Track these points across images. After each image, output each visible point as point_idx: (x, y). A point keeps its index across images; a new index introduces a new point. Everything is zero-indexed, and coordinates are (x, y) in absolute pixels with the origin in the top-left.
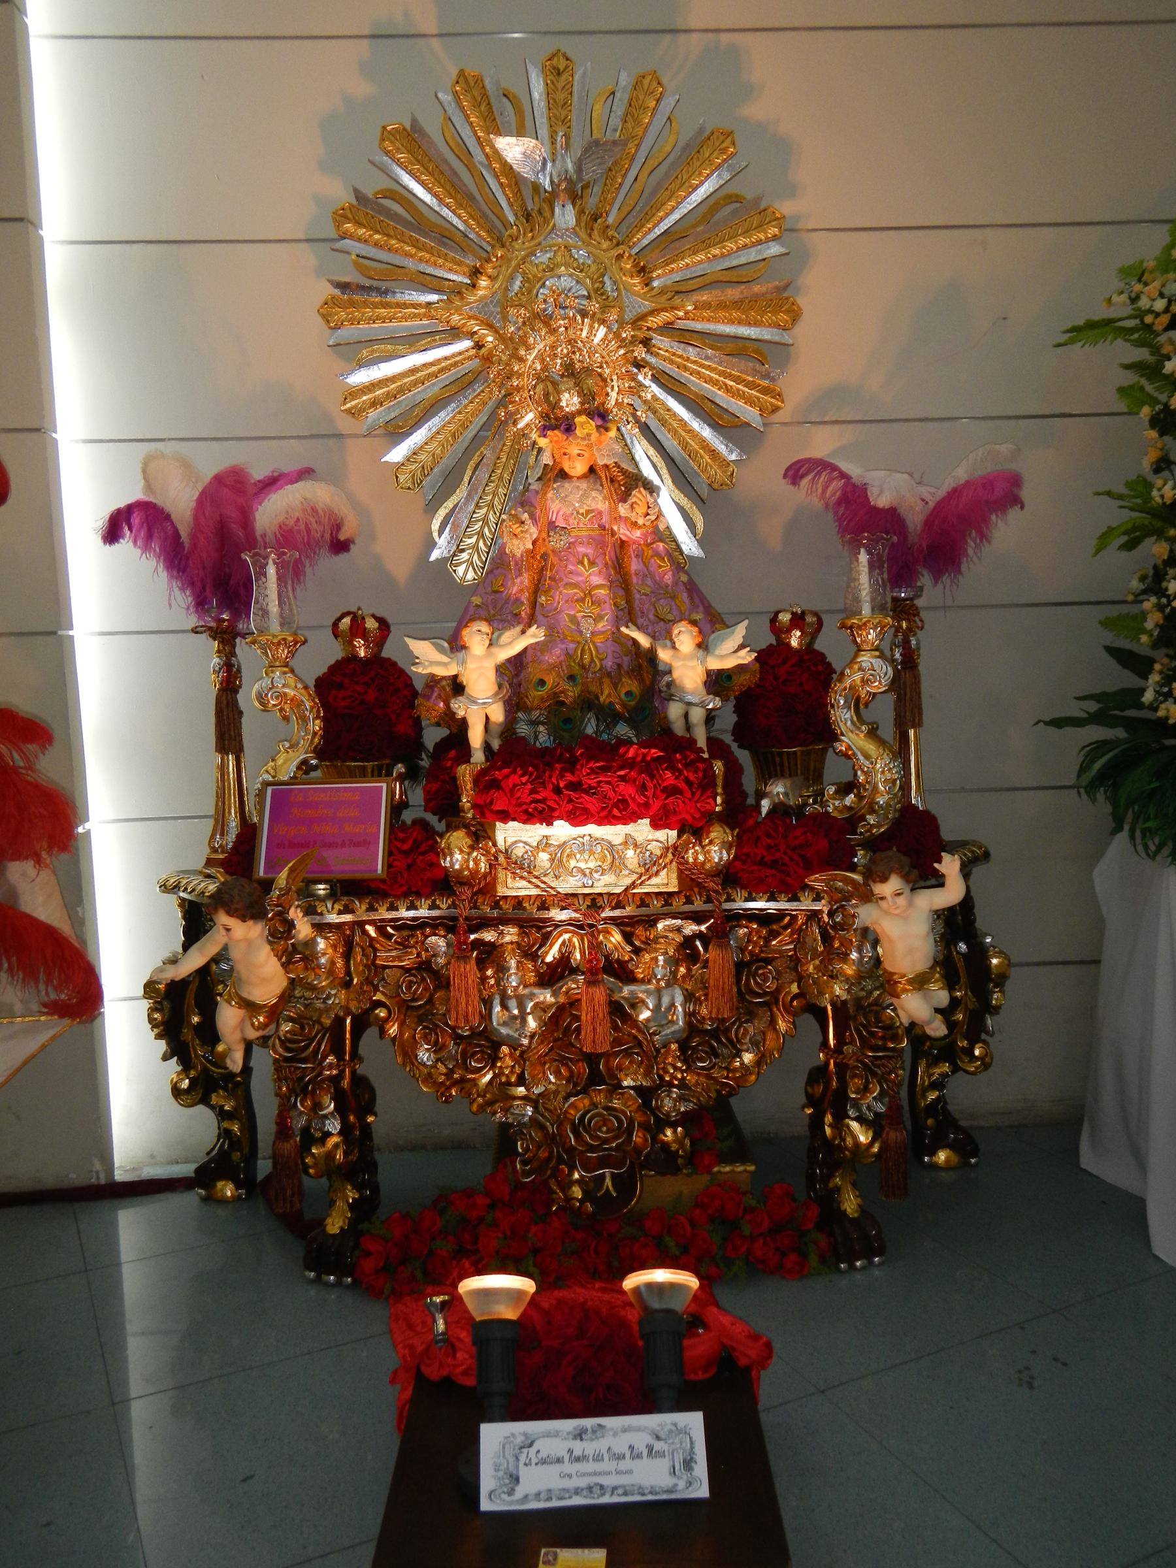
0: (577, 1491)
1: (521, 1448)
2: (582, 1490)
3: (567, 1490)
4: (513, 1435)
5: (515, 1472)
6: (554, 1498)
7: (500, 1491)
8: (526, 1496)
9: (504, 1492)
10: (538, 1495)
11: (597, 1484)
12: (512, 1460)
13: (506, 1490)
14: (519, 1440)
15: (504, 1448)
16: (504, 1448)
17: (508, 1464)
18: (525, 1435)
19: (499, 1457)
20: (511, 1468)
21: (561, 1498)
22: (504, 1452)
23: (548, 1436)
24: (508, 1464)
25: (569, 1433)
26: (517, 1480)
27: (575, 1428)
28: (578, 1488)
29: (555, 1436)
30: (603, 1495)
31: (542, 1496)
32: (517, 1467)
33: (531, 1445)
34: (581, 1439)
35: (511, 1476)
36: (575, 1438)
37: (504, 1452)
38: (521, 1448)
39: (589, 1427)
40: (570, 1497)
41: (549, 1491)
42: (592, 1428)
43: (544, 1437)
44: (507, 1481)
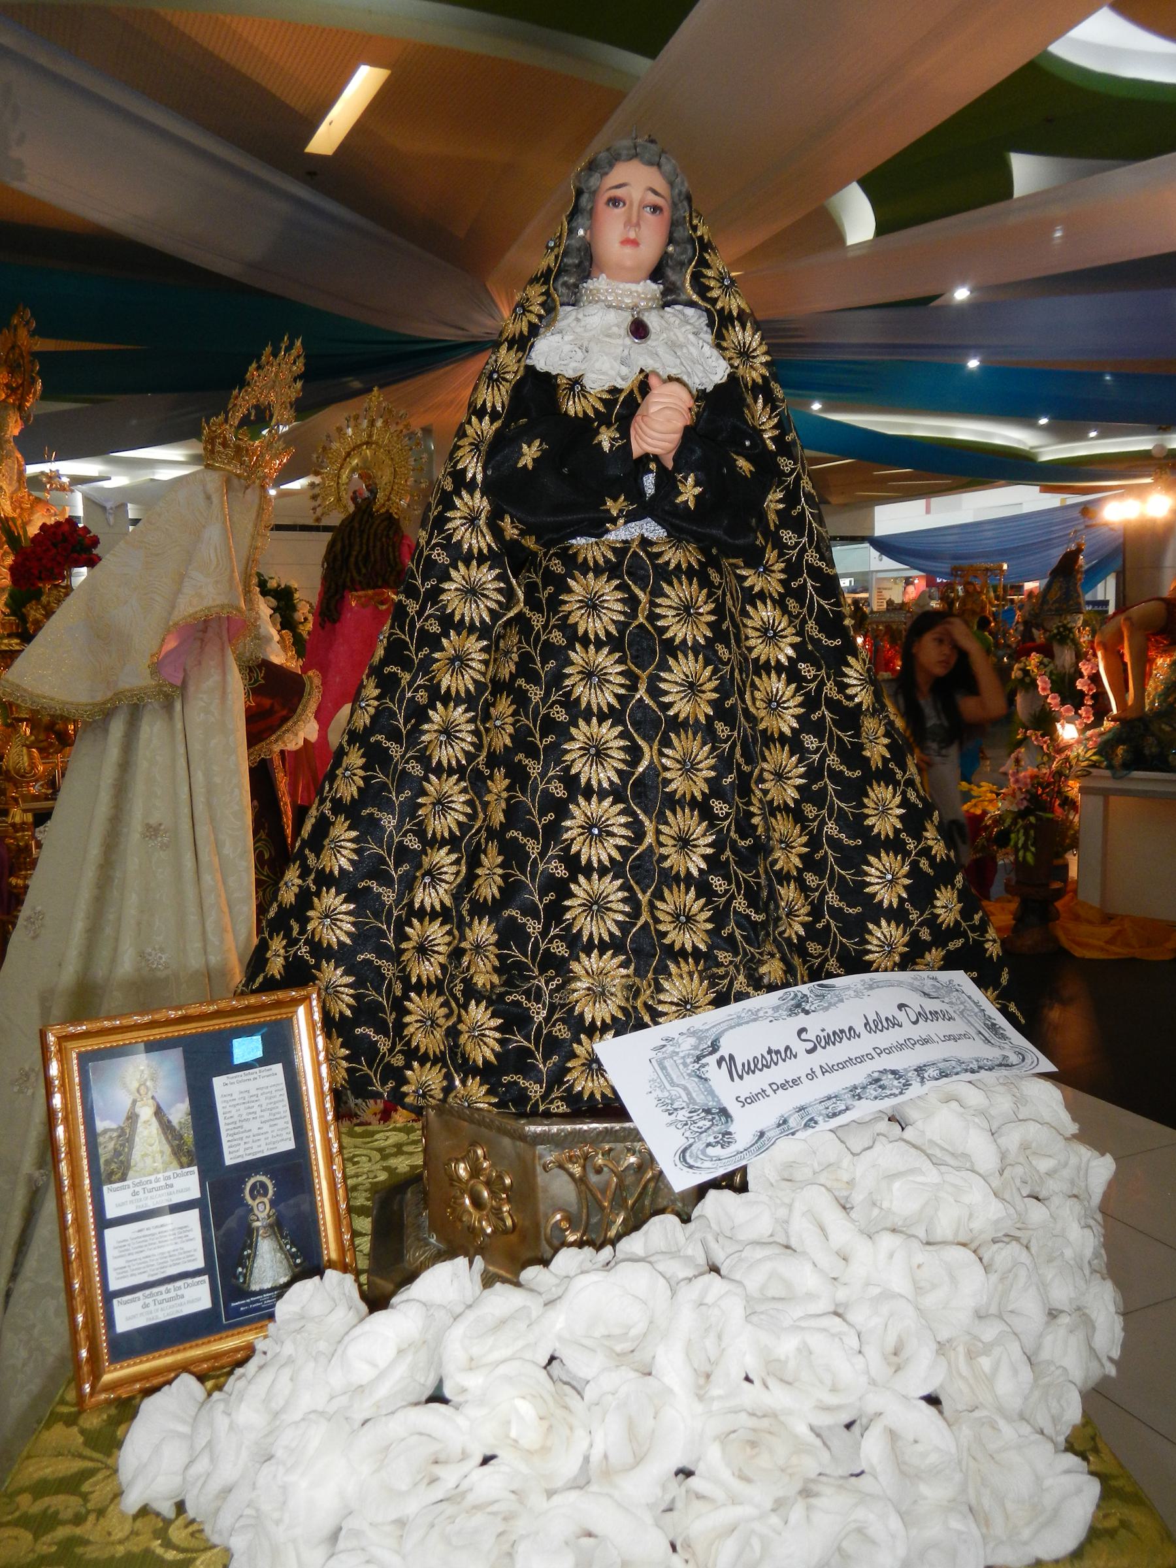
0: (856, 1093)
1: (699, 1058)
2: (864, 1088)
6: (820, 1119)
7: (700, 1145)
8: (762, 1134)
9: (709, 1145)
11: (884, 1072)
12: (693, 1084)
13: (711, 1140)
14: (688, 1044)
15: (663, 1068)
16: (663, 1068)
17: (685, 1089)
18: (692, 1033)
19: (663, 1088)
20: (701, 1099)
21: (835, 1115)
22: (667, 1075)
23: (739, 1025)
24: (685, 1089)
28: (855, 1088)
29: (755, 1020)
30: (907, 1085)
31: (792, 1122)
32: (711, 1092)
35: (708, 1111)
37: (667, 1075)
38: (698, 1059)
43: (732, 1027)
44: (708, 1124)
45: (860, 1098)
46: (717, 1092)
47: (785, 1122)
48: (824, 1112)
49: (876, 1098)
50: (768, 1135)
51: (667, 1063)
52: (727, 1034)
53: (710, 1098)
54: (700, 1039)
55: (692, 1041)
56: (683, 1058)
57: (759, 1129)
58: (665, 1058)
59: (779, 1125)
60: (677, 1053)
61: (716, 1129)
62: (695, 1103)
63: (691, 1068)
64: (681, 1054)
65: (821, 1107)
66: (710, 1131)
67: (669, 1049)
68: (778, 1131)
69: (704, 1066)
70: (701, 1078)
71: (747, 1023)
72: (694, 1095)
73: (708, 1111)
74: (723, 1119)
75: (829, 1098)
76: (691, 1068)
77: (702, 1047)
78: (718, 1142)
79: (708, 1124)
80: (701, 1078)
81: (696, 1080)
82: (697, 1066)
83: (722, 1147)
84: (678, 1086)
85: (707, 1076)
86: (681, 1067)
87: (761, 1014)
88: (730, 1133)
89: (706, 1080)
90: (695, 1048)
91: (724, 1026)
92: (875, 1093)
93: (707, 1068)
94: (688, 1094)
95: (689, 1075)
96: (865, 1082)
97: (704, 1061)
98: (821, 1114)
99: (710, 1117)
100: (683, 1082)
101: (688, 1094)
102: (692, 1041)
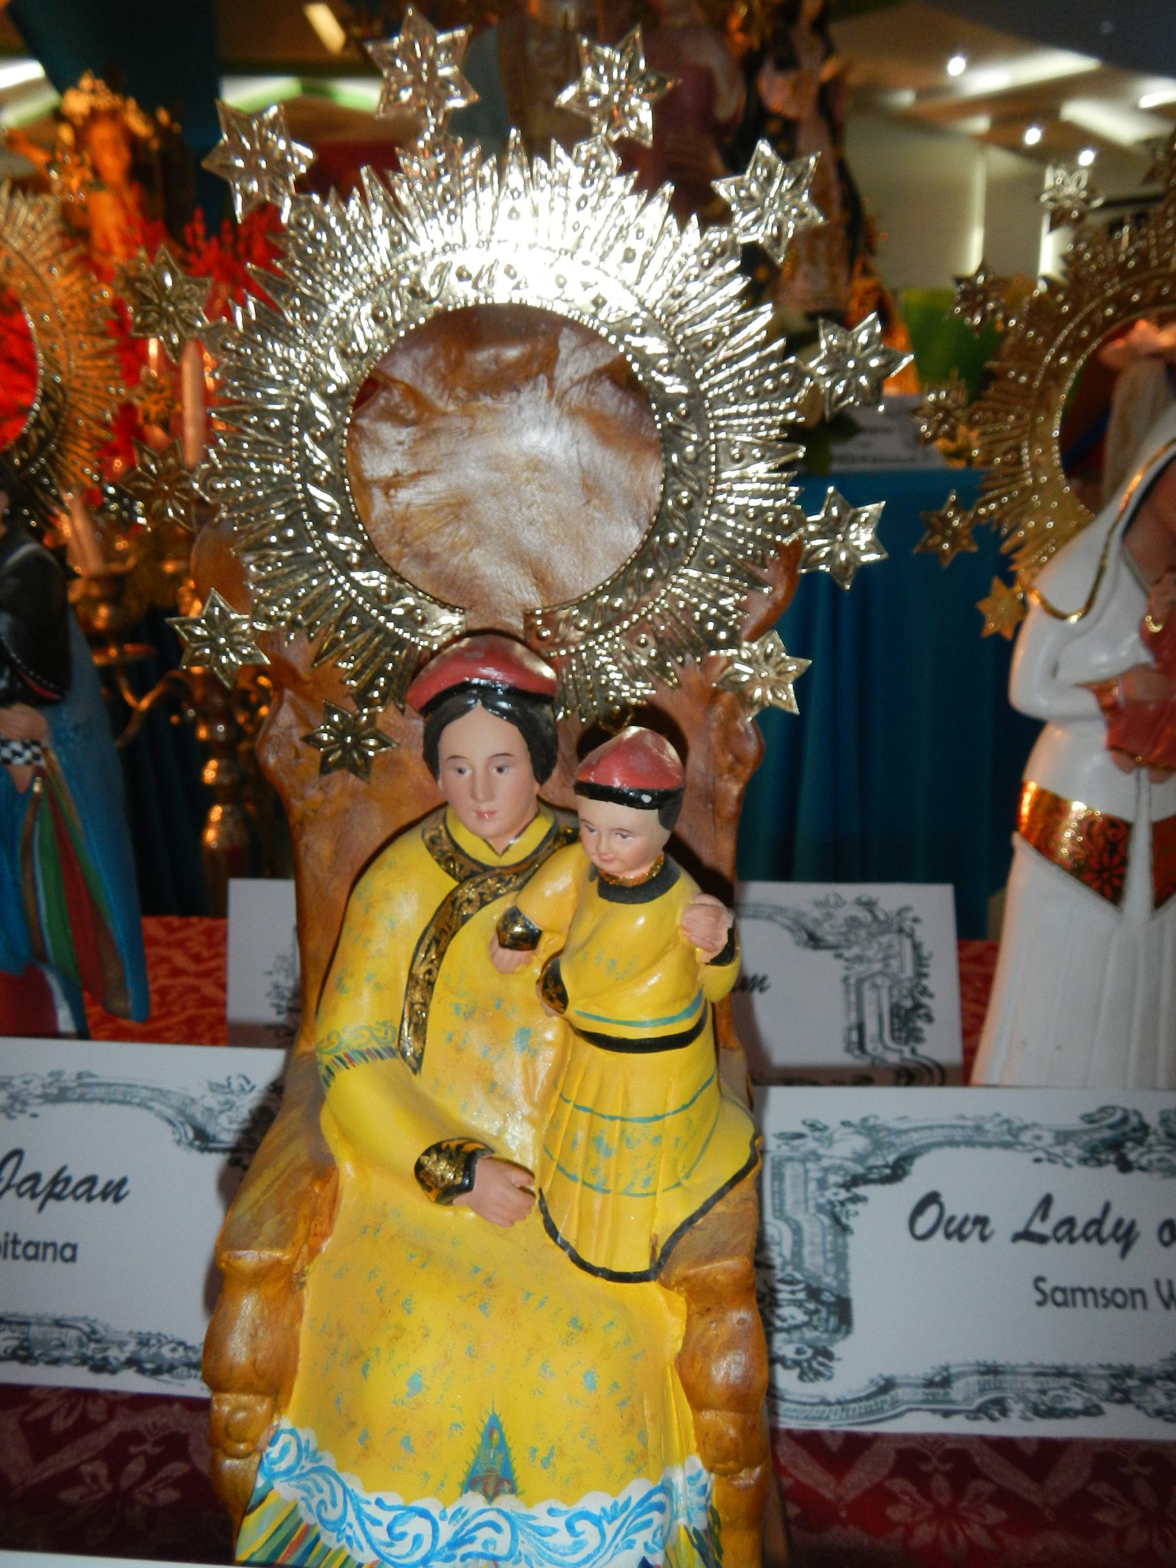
1: (856, 1181)
3: (1078, 1377)
4: (813, 1127)
5: (827, 1280)
6: (1016, 1408)
8: (888, 1386)
10: (942, 1381)
12: (815, 1228)
17: (797, 1231)
18: (867, 1128)
20: (814, 1261)
21: (1051, 1413)
23: (969, 1143)
24: (797, 1231)
25: (1063, 1137)
26: (842, 1310)
27: (1089, 1118)
28: (1129, 1372)
29: (1006, 1146)
31: (958, 1390)
32: (840, 1259)
33: (897, 1172)
34: (1125, 1166)
35: (814, 1293)
36: (1093, 1156)
38: (856, 1181)
39: (1152, 1120)
40: (1092, 1411)
41: (991, 1370)
42: (1165, 1120)
43: (952, 1143)
44: (800, 1317)
45: (1126, 1399)
46: (855, 1264)
47: (946, 1382)
48: (1033, 1397)
49: (1159, 1413)
50: (901, 1393)
51: (789, 1171)
52: (936, 1155)
53: (832, 1269)
54: (878, 1145)
55: (860, 1143)
56: (826, 1170)
57: (888, 1372)
58: (790, 1159)
59: (930, 1383)
60: (818, 1158)
61: (809, 1334)
62: (799, 1266)
63: (829, 1194)
64: (826, 1163)
65: (1032, 1384)
66: (796, 1335)
67: (810, 1144)
68: (920, 1394)
69: (856, 1199)
70: (836, 1220)
71: (988, 1145)
72: (807, 1250)
73: (814, 1293)
74: (833, 1321)
75: (1060, 1372)
76: (829, 1194)
77: (872, 1161)
78: (797, 1363)
79: (800, 1317)
80: (836, 1220)
81: (827, 1221)
82: (843, 1194)
83: (801, 1377)
84: (787, 1220)
85: (852, 1222)
86: (813, 1186)
87: (1026, 1137)
88: (829, 1356)
89: (845, 1229)
90: (859, 1158)
91: (938, 1135)
92: (1162, 1401)
93: (859, 1207)
94: (798, 1243)
95: (820, 1208)
96: (1157, 1369)
97: (861, 1190)
98: (1022, 1398)
99: (811, 1306)
100: (801, 1217)
101: (798, 1243)
102: (860, 1143)
